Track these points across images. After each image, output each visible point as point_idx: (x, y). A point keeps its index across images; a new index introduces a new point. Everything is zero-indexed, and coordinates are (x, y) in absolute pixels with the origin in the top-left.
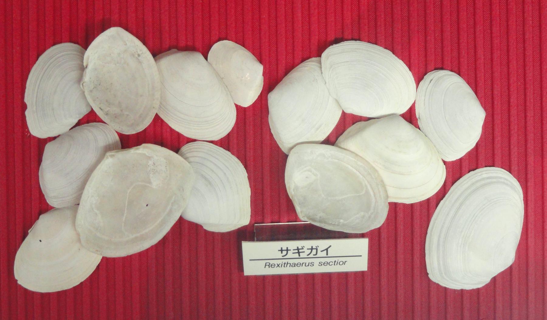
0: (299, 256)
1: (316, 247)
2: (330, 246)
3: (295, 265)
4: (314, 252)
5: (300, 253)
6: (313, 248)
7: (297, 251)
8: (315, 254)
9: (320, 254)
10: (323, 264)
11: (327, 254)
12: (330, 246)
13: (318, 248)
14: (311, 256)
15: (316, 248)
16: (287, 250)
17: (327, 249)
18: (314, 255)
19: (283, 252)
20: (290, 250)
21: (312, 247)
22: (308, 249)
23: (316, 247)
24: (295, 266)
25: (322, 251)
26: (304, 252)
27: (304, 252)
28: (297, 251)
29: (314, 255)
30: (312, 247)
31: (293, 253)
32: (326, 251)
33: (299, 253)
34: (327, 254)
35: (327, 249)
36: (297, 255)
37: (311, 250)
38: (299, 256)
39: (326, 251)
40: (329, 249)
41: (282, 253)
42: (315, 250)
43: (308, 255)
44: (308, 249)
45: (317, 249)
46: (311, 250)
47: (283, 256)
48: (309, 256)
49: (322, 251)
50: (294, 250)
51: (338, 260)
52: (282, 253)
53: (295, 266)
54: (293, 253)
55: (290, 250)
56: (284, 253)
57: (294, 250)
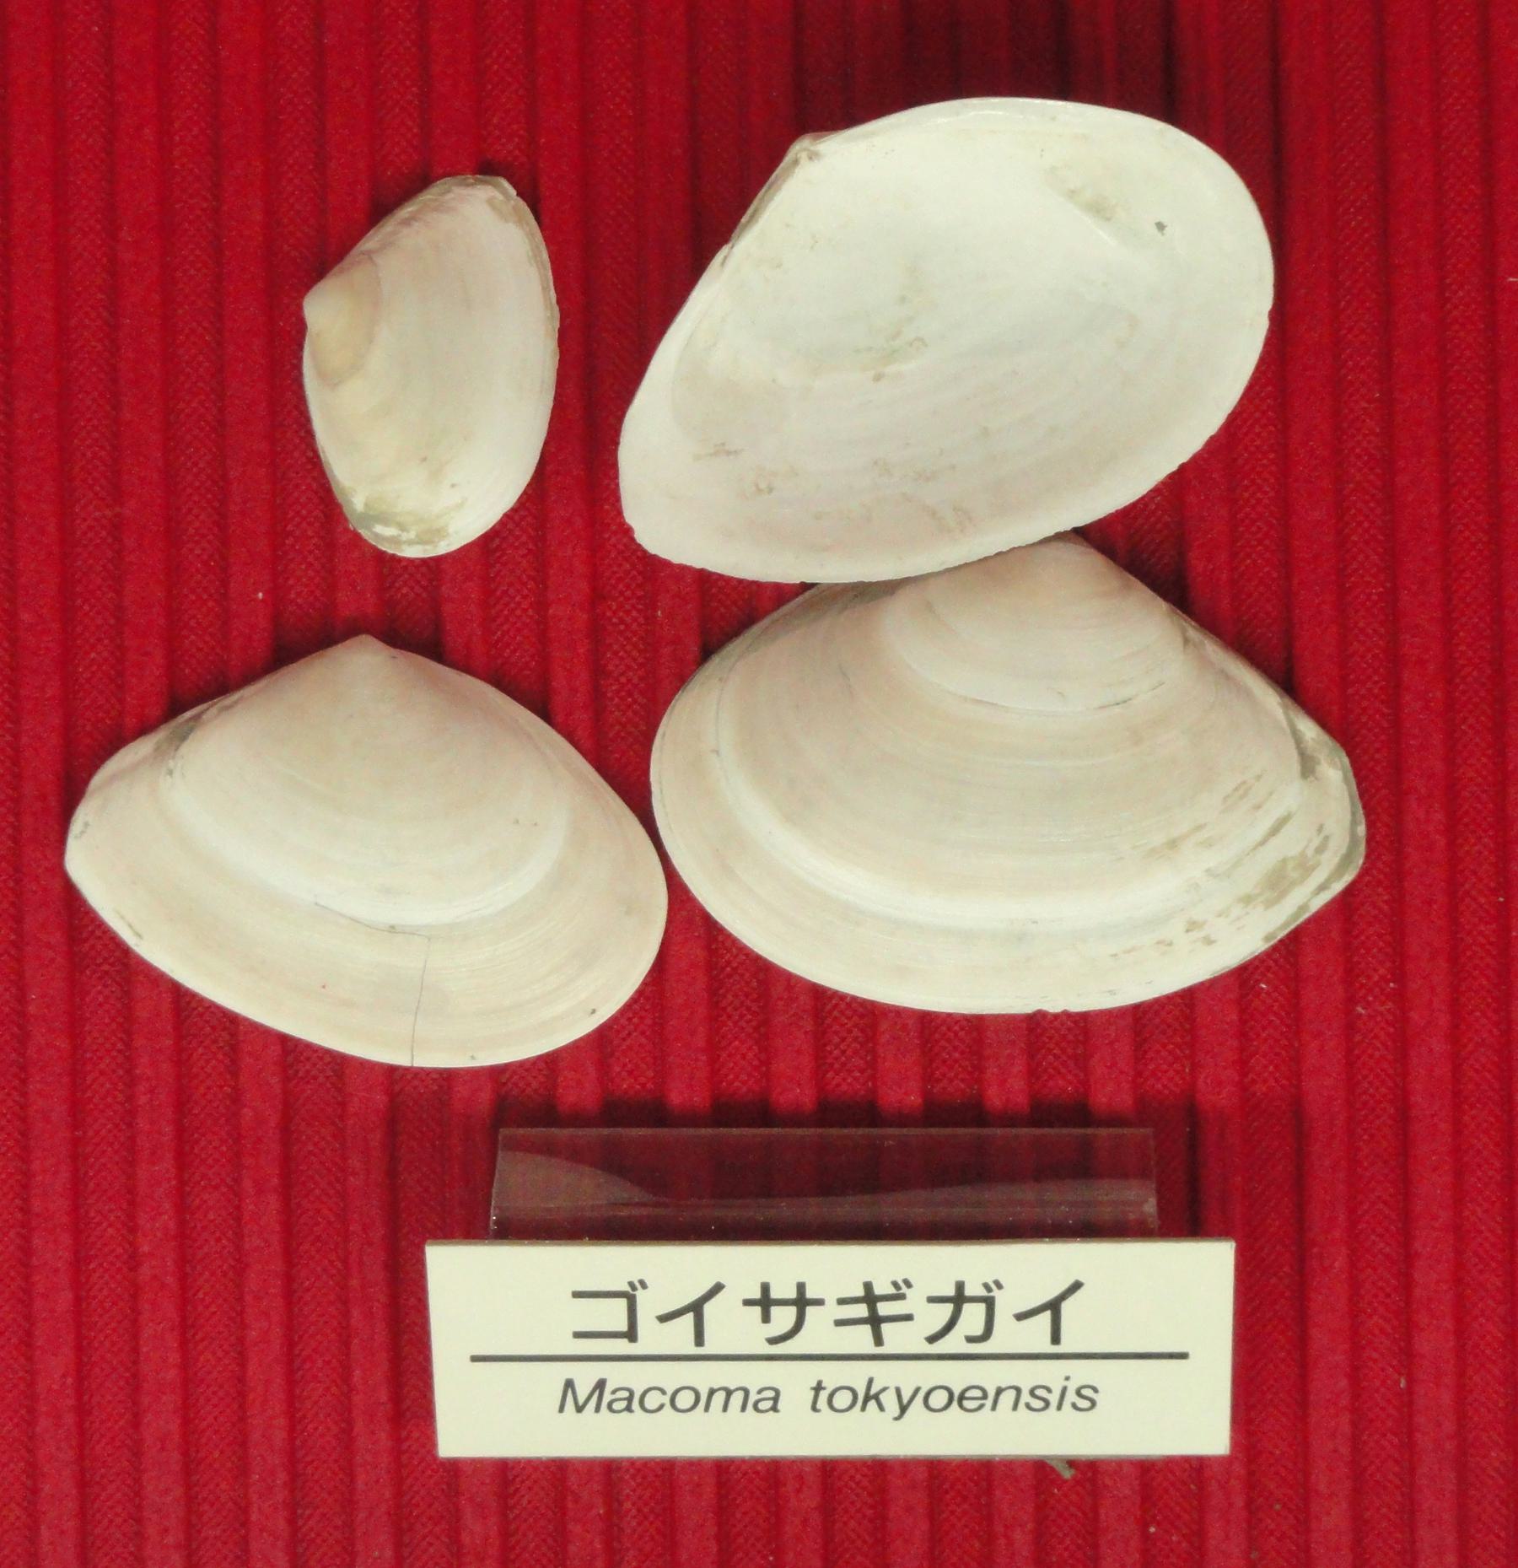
0: (879, 1341)
1: (987, 1287)
2: (1076, 1286)
5: (886, 1328)
6: (968, 1292)
7: (862, 1311)
8: (978, 1330)
9: (1008, 1335)
10: (1026, 1397)
11: (1056, 1338)
12: (1076, 1286)
13: (996, 1293)
14: (954, 1343)
15: (983, 1293)
16: (802, 1302)
17: (1054, 1306)
19: (775, 1311)
20: (819, 1302)
21: (960, 1286)
22: (932, 1300)
23: (987, 1287)
25: (1021, 1317)
26: (908, 1318)
27: (908, 1318)
28: (862, 1311)
29: (971, 1340)
30: (960, 1286)
31: (840, 1323)
32: (1047, 1315)
33: (875, 1321)
34: (1056, 1338)
35: (1054, 1306)
36: (860, 1339)
37: (949, 1307)
38: (879, 1341)
39: (1047, 1315)
40: (1066, 1307)
41: (766, 1318)
42: (982, 1307)
43: (932, 1339)
44: (932, 1300)
45: (990, 1303)
46: (948, 1308)
47: (773, 1341)
48: (941, 1347)
49: (1021, 1317)
50: (842, 1302)
51: (1067, 1378)
52: (766, 1318)
54: (840, 1323)
55: (819, 1302)
56: (784, 1318)
57: (842, 1302)
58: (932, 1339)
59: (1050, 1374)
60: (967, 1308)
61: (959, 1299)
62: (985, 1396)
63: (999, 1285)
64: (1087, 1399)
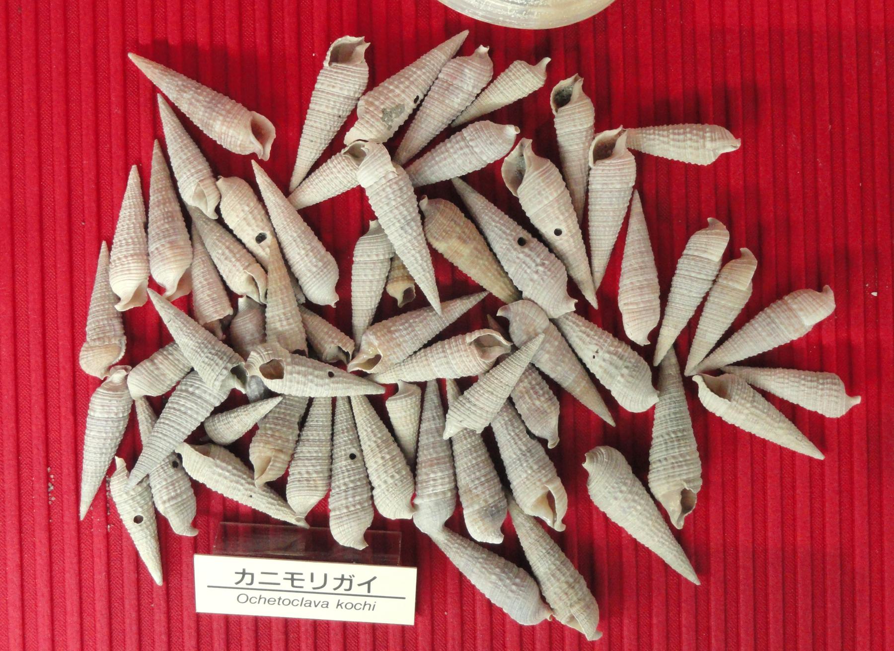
2: (375, 578)
3: (310, 603)
4: (346, 584)
6: (345, 577)
9: (355, 590)
11: (369, 591)
12: (375, 578)
18: (346, 590)
21: (343, 576)
22: (335, 579)
24: (310, 606)
25: (359, 585)
29: (346, 590)
30: (343, 576)
34: (369, 591)
35: (369, 583)
37: (340, 581)
40: (372, 583)
42: (349, 582)
43: (335, 589)
44: (335, 579)
45: (351, 581)
49: (359, 585)
53: (310, 606)
58: (335, 589)
61: (342, 579)
64: (372, 608)
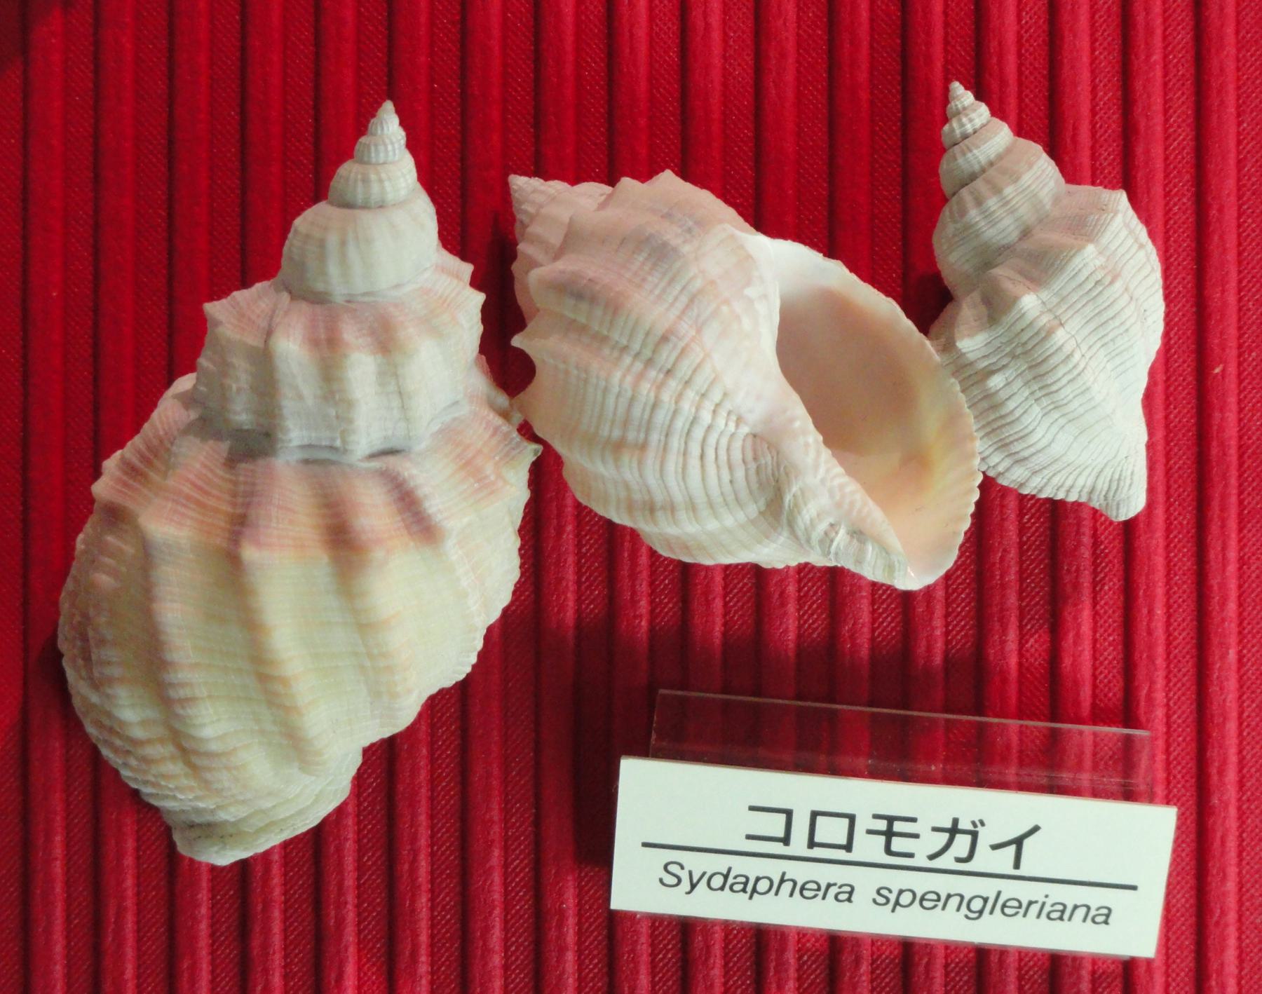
2: (1036, 829)
4: (962, 843)
6: (961, 826)
8: (964, 854)
11: (1017, 865)
12: (1036, 829)
13: (980, 828)
14: (946, 861)
15: (971, 827)
17: (1018, 842)
18: (959, 860)
21: (956, 821)
22: (935, 829)
25: (995, 847)
29: (959, 860)
30: (956, 821)
32: (1013, 848)
34: (1017, 865)
35: (1018, 842)
37: (946, 836)
39: (1013, 848)
40: (1027, 843)
42: (968, 838)
45: (974, 835)
46: (946, 836)
48: (936, 863)
49: (995, 847)
58: (932, 857)
59: (1011, 889)
60: (958, 837)
61: (954, 830)
62: (939, 900)
63: (982, 824)
